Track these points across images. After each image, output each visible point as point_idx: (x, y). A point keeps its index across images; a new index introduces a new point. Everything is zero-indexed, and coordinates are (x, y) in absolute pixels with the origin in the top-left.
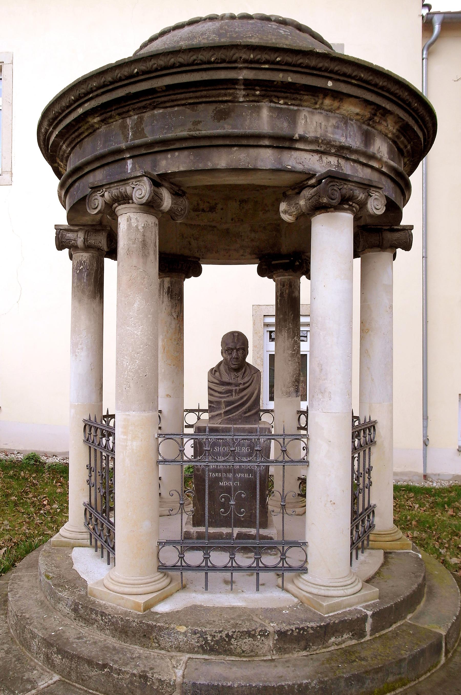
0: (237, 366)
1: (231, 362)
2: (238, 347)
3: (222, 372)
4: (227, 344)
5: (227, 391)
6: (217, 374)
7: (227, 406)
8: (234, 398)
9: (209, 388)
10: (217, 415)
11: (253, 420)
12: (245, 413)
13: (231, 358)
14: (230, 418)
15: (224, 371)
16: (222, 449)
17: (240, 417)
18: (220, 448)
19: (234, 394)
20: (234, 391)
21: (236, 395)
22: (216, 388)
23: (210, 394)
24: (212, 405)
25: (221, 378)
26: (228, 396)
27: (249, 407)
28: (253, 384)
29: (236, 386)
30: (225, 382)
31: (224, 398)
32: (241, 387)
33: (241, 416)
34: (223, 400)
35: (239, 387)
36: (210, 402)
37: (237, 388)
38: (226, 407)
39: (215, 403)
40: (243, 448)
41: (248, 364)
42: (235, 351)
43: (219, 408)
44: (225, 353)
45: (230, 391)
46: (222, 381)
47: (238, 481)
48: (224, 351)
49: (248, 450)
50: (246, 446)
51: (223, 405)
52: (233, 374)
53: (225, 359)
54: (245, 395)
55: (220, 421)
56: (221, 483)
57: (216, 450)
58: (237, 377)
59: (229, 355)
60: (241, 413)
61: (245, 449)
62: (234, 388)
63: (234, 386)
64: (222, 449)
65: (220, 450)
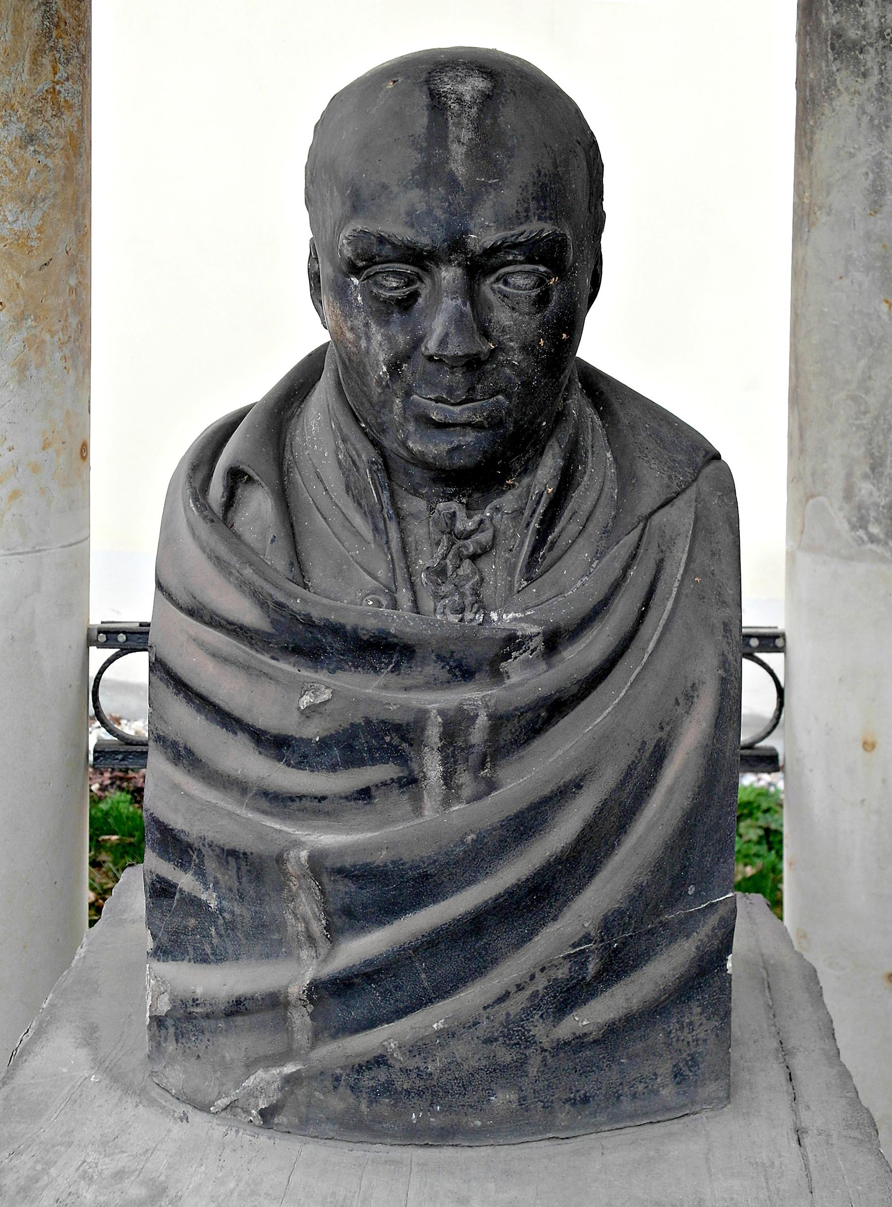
0: (470, 437)
1: (408, 394)
5: (353, 731)
11: (665, 1068)
13: (407, 357)
14: (380, 1061)
20: (433, 734)
21: (464, 778)
26: (365, 794)
30: (336, 630)
35: (497, 676)
46: (294, 616)
48: (326, 271)
63: (433, 669)
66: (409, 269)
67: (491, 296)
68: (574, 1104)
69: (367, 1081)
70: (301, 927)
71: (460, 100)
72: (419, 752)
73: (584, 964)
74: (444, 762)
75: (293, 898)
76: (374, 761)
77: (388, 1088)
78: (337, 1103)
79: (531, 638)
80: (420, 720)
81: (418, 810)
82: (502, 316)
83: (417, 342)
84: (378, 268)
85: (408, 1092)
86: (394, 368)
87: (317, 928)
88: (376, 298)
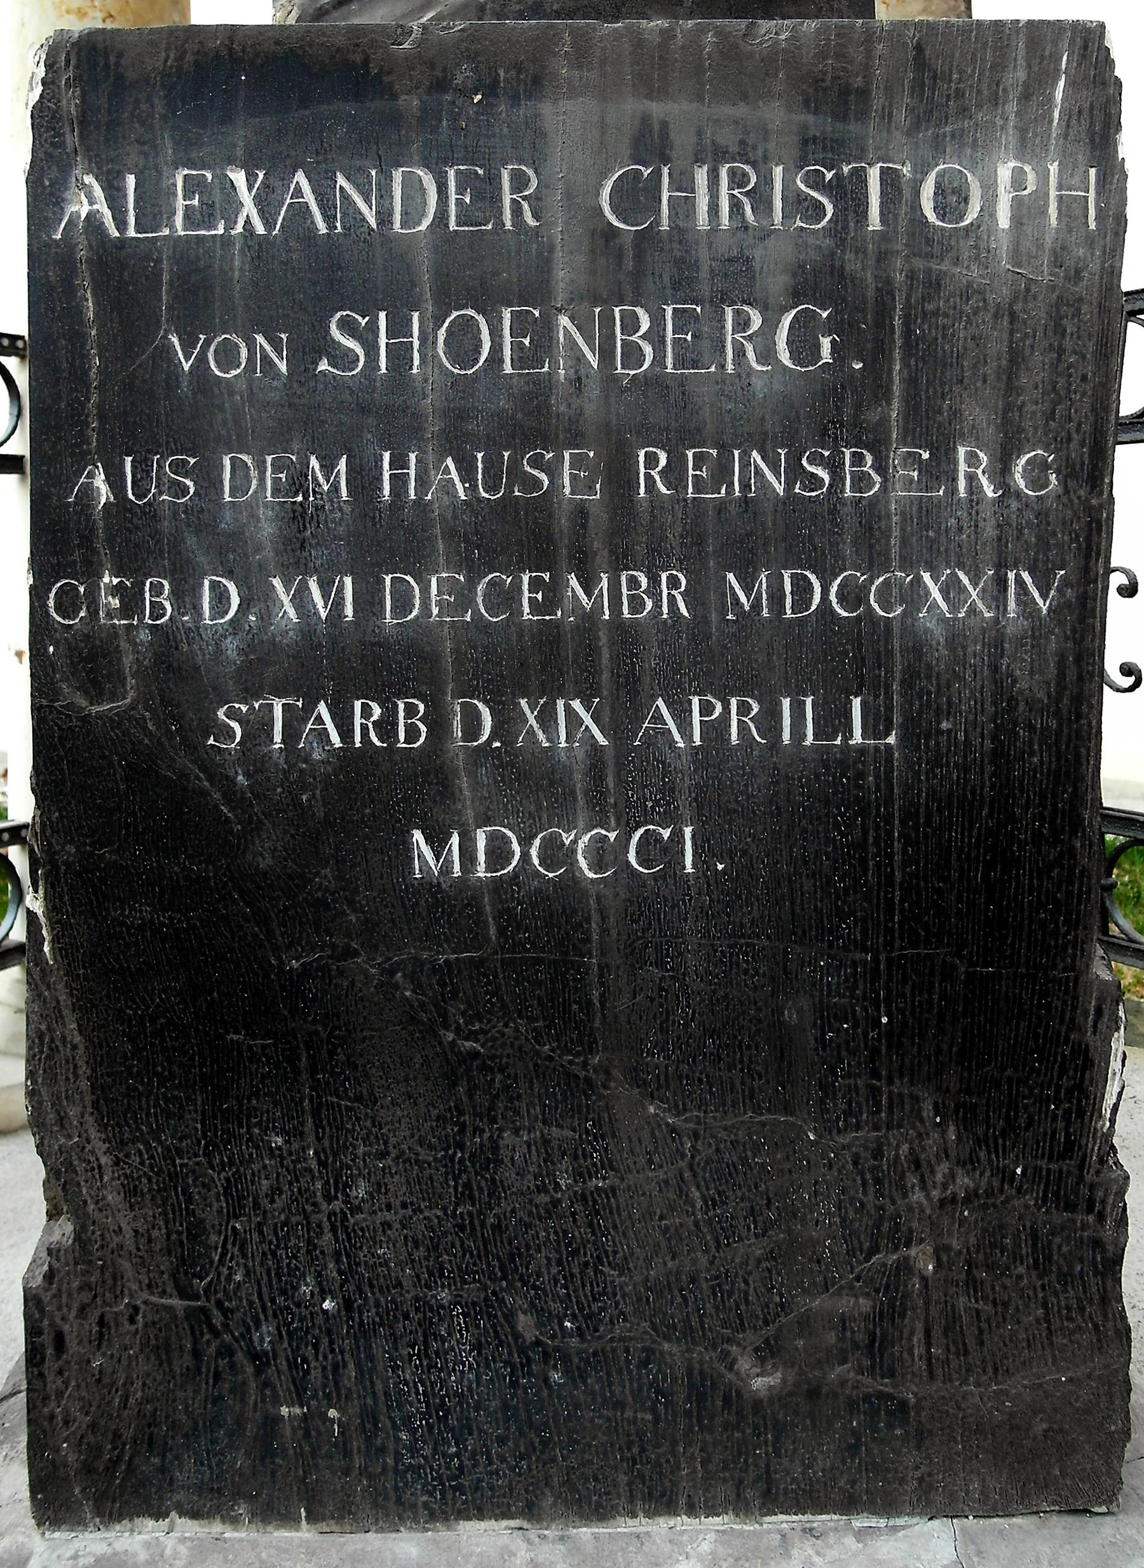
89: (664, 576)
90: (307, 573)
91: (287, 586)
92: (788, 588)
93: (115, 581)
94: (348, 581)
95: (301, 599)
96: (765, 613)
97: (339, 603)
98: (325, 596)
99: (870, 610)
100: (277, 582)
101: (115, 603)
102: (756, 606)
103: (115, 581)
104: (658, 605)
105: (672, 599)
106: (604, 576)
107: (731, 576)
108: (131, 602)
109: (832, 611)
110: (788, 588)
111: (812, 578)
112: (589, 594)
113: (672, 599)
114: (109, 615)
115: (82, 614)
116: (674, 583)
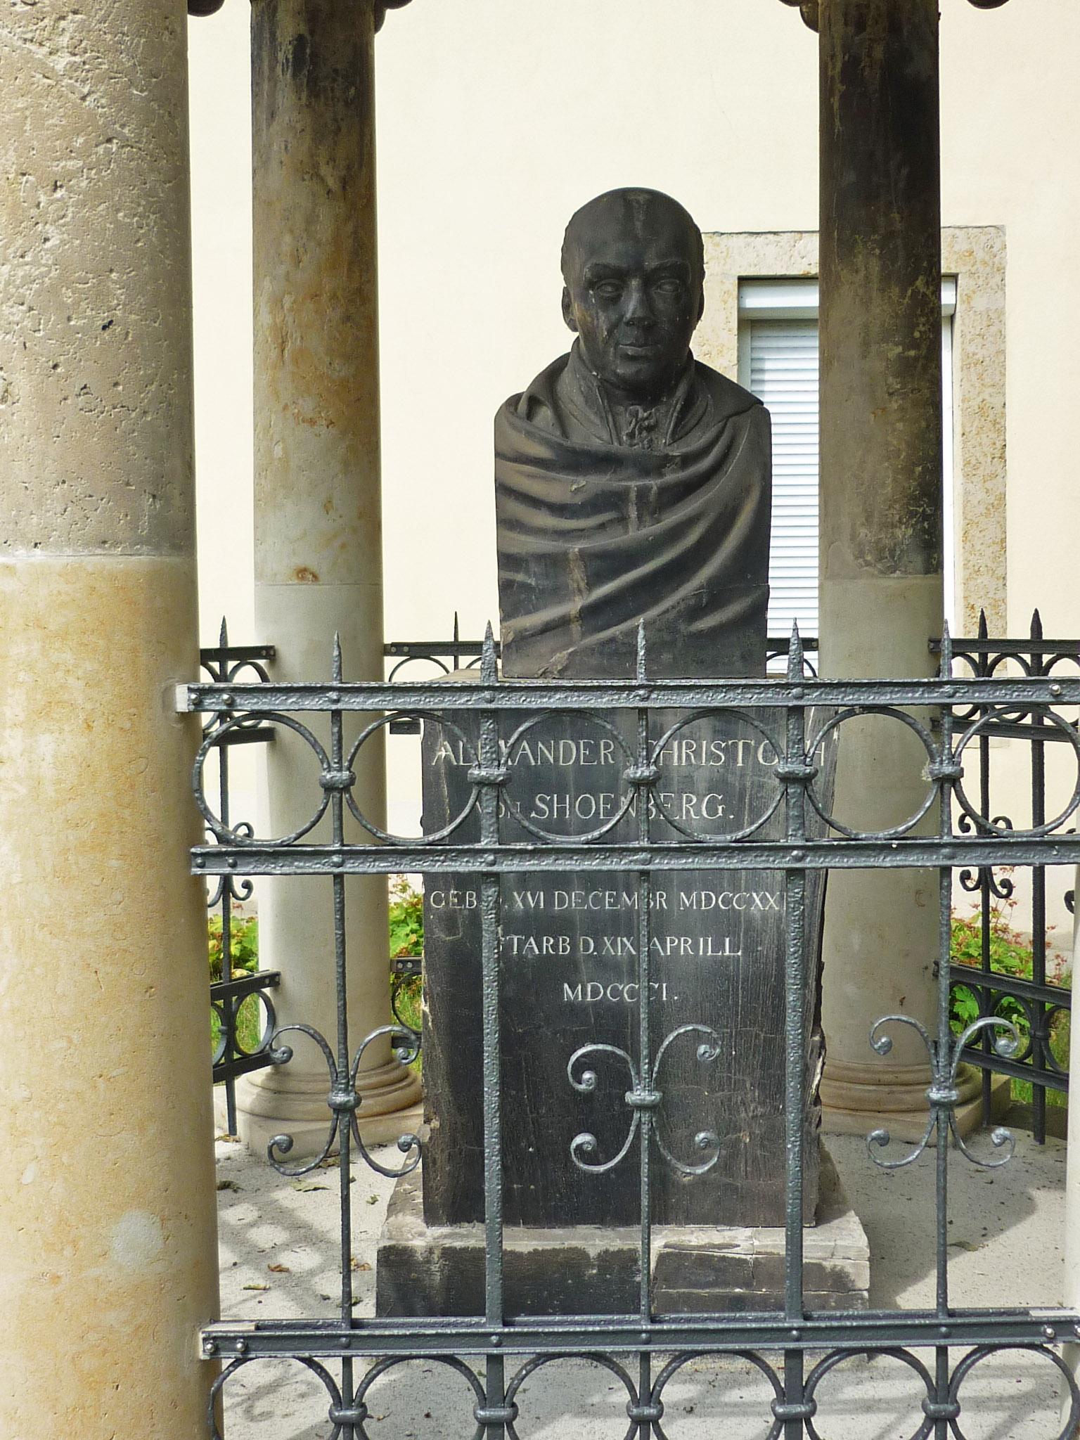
1: (617, 344)
2: (651, 263)
3: (567, 407)
4: (592, 252)
6: (545, 414)
7: (595, 579)
8: (635, 533)
9: (503, 490)
10: (547, 628)
12: (695, 611)
14: (612, 640)
15: (579, 400)
16: (572, 805)
17: (667, 637)
18: (561, 800)
19: (633, 513)
20: (633, 495)
22: (536, 488)
23: (505, 523)
24: (520, 577)
25: (565, 434)
26: (602, 526)
27: (712, 582)
28: (731, 468)
29: (645, 472)
31: (580, 537)
32: (672, 476)
33: (672, 628)
34: (576, 547)
36: (507, 560)
37: (654, 483)
38: (591, 586)
39: (534, 567)
40: (689, 801)
41: (704, 372)
42: (634, 283)
43: (557, 593)
44: (584, 298)
45: (611, 501)
47: (663, 976)
49: (712, 810)
50: (702, 786)
51: (577, 575)
52: (630, 415)
53: (588, 336)
54: (690, 522)
55: (561, 657)
56: (573, 988)
57: (541, 812)
58: (650, 429)
59: (605, 309)
60: (671, 615)
61: (700, 801)
62: (634, 484)
64: (572, 805)
65: (561, 811)
66: (617, 282)
67: (654, 295)
68: (697, 663)
69: (606, 650)
70: (575, 586)
71: (638, 202)
72: (627, 506)
73: (701, 599)
74: (638, 510)
75: (571, 572)
76: (606, 511)
77: (616, 653)
78: (594, 661)
79: (676, 456)
80: (627, 489)
81: (626, 532)
82: (660, 305)
83: (622, 316)
84: (603, 282)
85: (625, 653)
86: (610, 332)
87: (583, 585)
88: (602, 297)
89: (658, 893)
90: (527, 890)
91: (519, 894)
92: (703, 898)
93: (456, 892)
94: (542, 893)
95: (524, 900)
96: (695, 907)
97: (538, 903)
98: (533, 899)
99: (733, 906)
100: (515, 894)
101: (456, 900)
102: (691, 905)
103: (456, 892)
104: (655, 904)
105: (660, 902)
106: (636, 893)
107: (682, 894)
108: (461, 900)
109: (719, 907)
110: (703, 898)
111: (712, 894)
112: (630, 900)
113: (660, 902)
114: (453, 905)
115: (443, 904)
116: (661, 896)
